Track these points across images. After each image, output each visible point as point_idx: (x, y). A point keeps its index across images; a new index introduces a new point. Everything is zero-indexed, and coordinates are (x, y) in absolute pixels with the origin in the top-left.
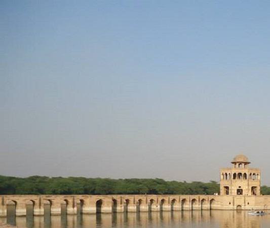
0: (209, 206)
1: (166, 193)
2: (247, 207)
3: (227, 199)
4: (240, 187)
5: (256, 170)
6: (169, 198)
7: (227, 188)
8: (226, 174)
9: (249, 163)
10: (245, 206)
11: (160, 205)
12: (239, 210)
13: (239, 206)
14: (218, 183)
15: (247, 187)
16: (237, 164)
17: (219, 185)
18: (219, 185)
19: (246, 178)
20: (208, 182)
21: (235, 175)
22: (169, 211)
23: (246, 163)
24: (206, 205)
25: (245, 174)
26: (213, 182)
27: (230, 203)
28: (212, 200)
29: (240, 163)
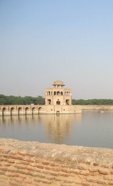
0: (38, 111)
1: (6, 104)
2: (64, 112)
3: (50, 107)
4: (58, 100)
5: (69, 89)
6: (9, 107)
7: (50, 100)
8: (49, 92)
9: (64, 85)
10: (62, 111)
11: (2, 112)
12: (58, 114)
13: (58, 111)
14: (43, 98)
15: (63, 100)
16: (57, 86)
17: (45, 99)
18: (45, 99)
19: (62, 95)
20: (37, 97)
21: (55, 92)
22: (9, 115)
23: (62, 86)
24: (36, 111)
25: (62, 92)
26: (40, 97)
27: (52, 110)
28: (40, 108)
29: (58, 86)
